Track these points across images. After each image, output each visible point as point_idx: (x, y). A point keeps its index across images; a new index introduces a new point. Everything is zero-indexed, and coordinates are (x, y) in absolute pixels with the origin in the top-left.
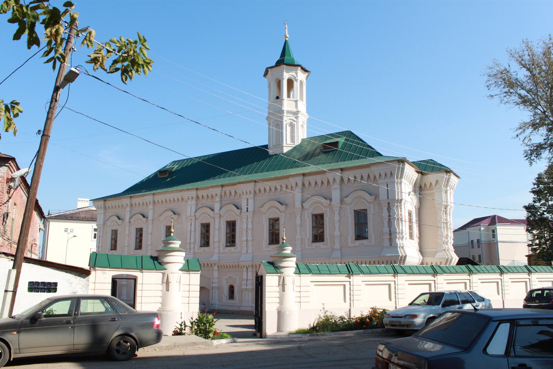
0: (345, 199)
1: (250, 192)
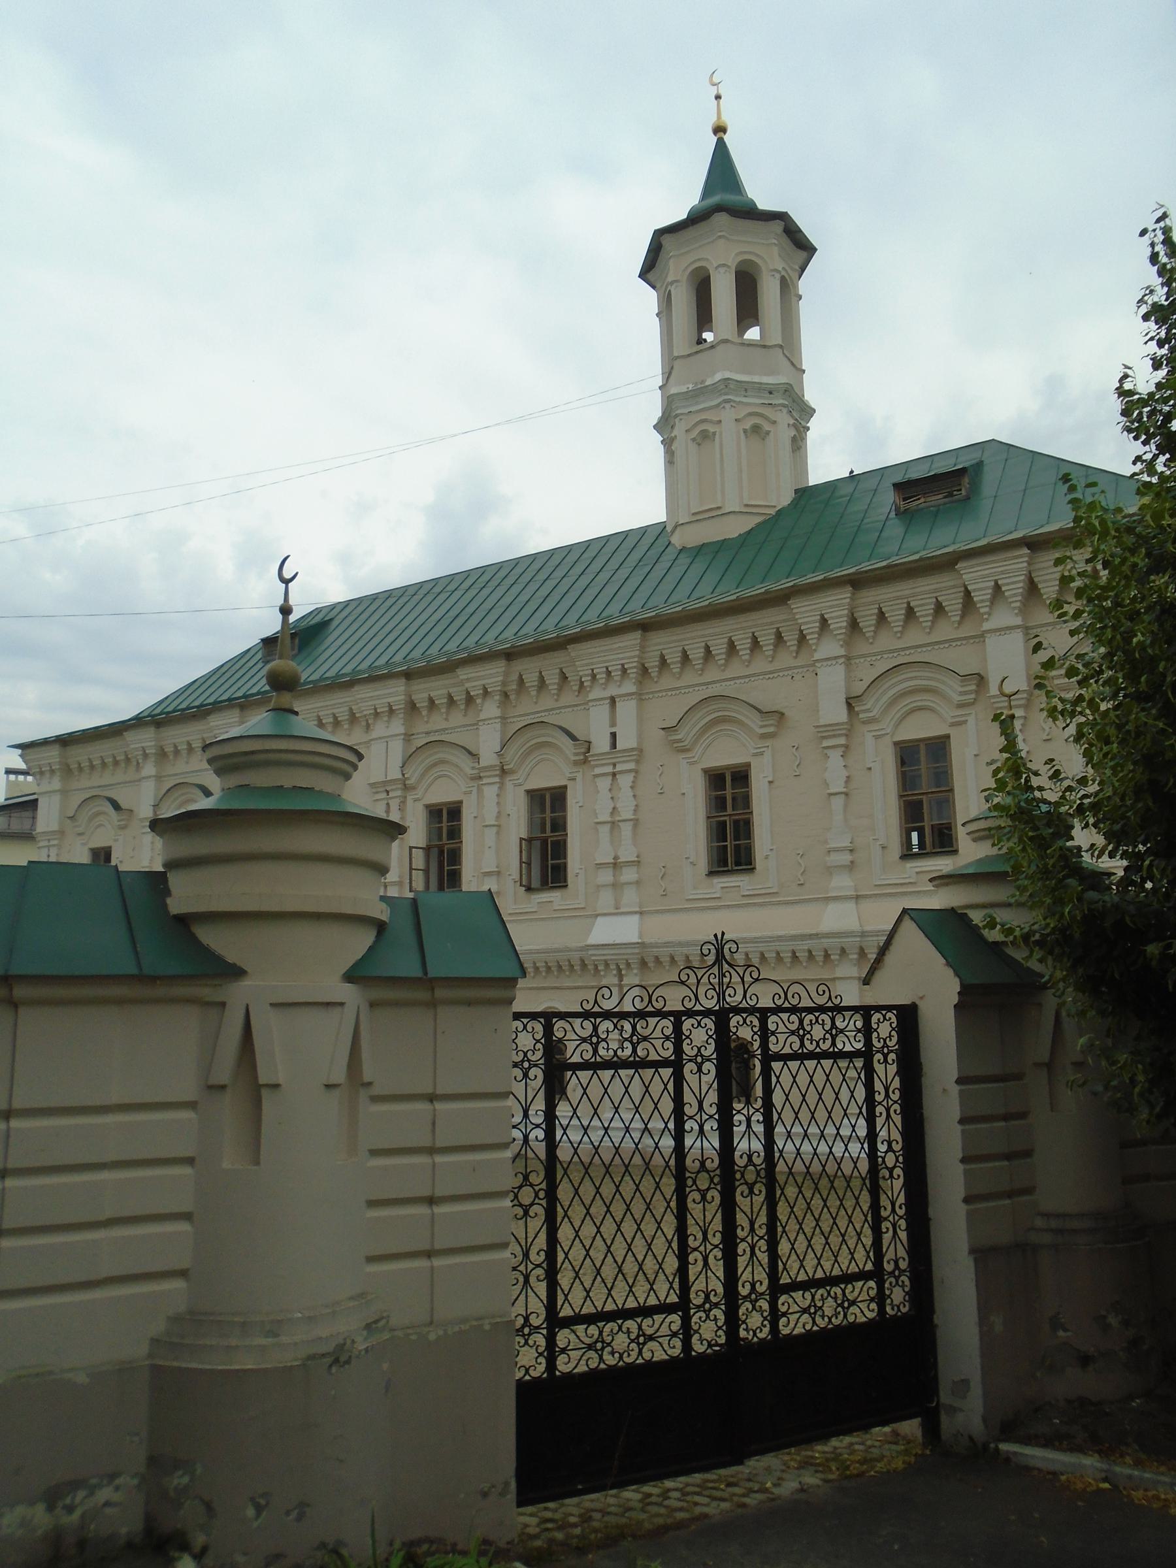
1: (624, 671)
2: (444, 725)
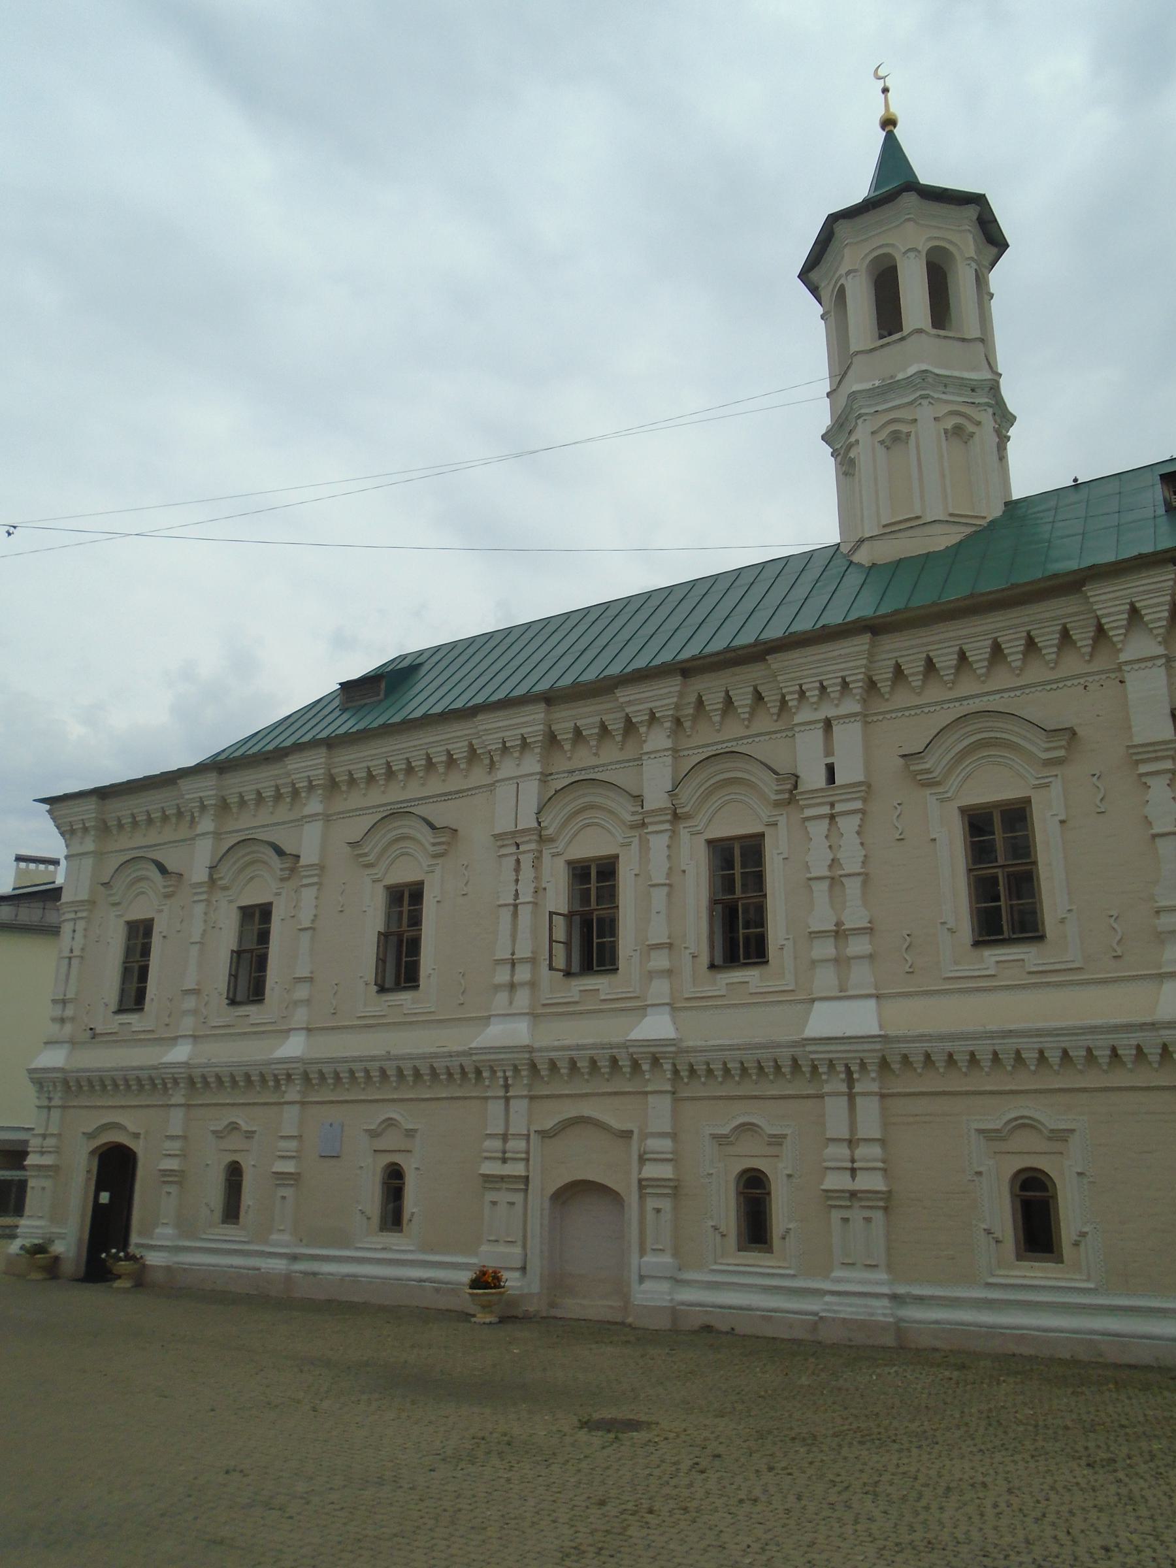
1: (845, 684)
2: (594, 761)
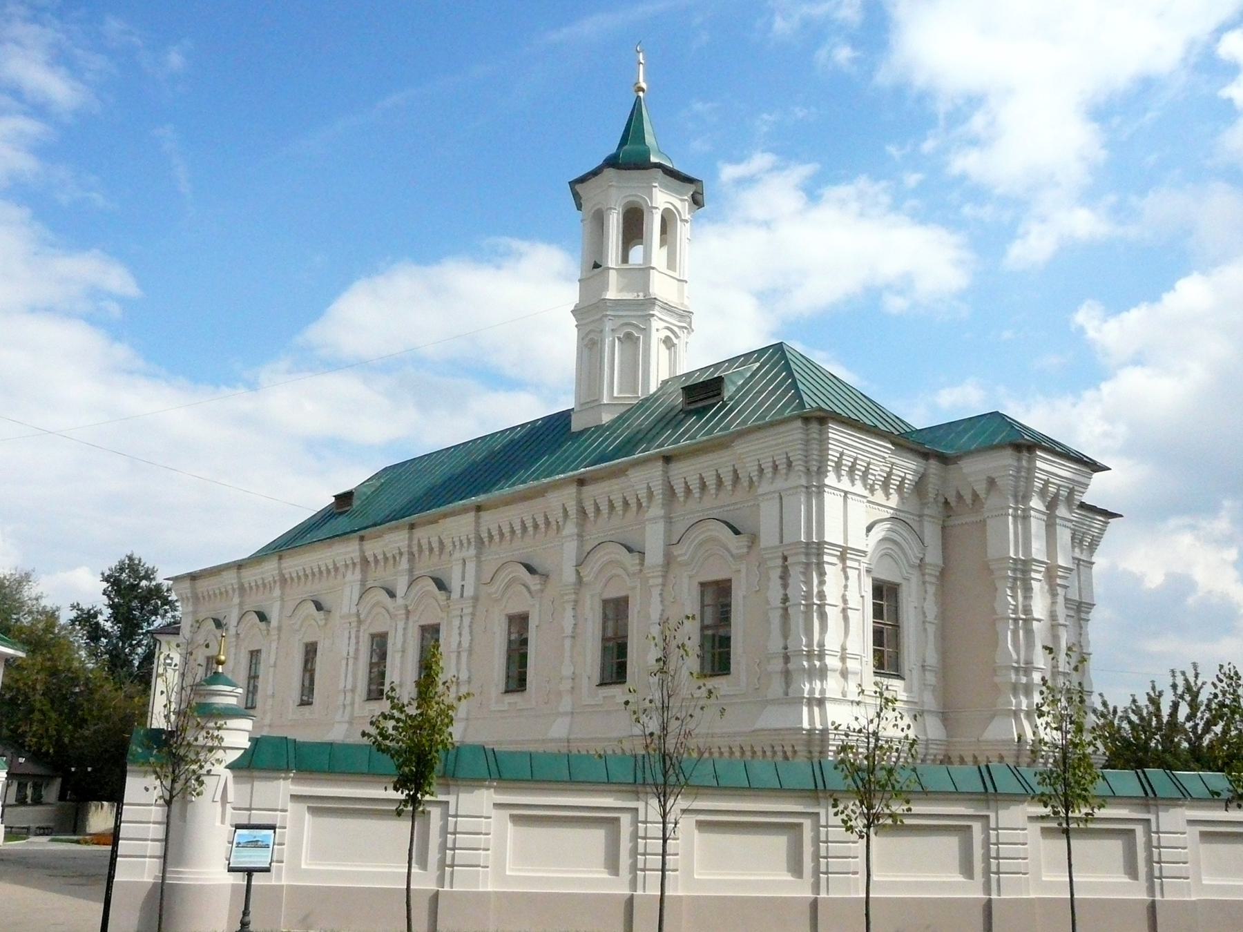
0: (677, 551)
